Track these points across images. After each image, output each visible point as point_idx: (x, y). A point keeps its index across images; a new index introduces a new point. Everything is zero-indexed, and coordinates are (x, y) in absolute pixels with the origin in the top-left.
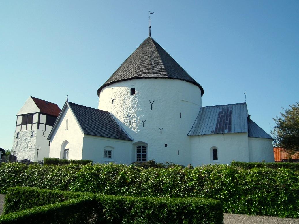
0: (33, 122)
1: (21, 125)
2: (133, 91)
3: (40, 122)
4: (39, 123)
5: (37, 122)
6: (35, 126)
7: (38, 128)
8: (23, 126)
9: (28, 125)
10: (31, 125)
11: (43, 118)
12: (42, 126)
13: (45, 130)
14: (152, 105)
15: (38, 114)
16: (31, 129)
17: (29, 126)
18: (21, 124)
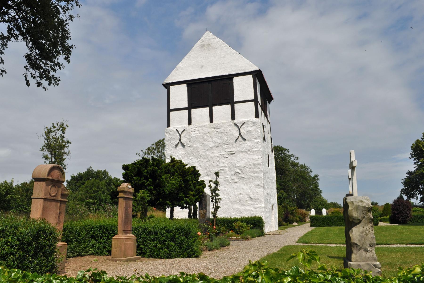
0: (236, 99)
3: (253, 103)
5: (253, 97)
7: (257, 116)
8: (193, 111)
9: (215, 108)
10: (228, 107)
15: (250, 77)
16: (233, 118)
18: (186, 106)
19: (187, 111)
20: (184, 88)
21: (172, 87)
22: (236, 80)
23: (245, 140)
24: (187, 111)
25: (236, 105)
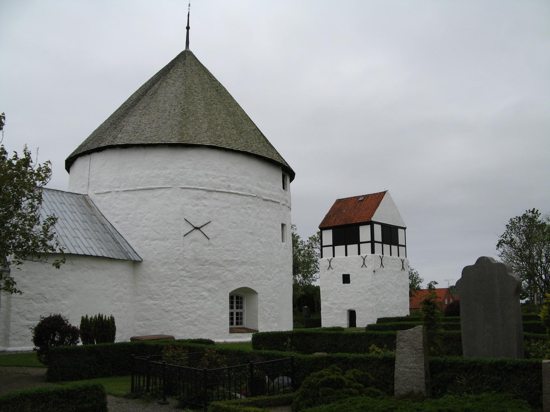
0: (361, 240)
1: (333, 246)
4: (373, 242)
5: (370, 240)
6: (366, 248)
7: (373, 252)
9: (348, 246)
10: (357, 245)
13: (383, 254)
16: (359, 254)
17: (353, 248)
18: (332, 244)
19: (332, 247)
24: (332, 247)
25: (361, 245)
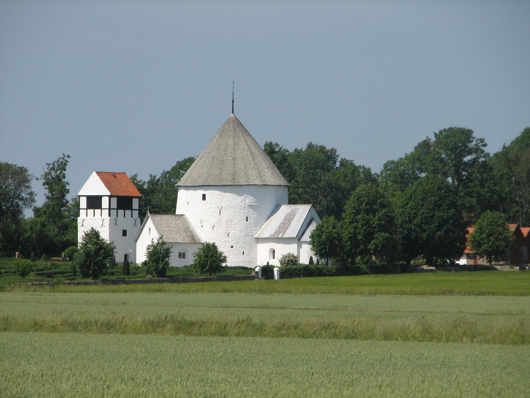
1: (87, 209)
2: (204, 197)
4: (110, 209)
5: (108, 207)
6: (106, 212)
7: (109, 215)
8: (88, 210)
10: (100, 210)
11: (114, 201)
12: (114, 212)
13: (117, 216)
14: (220, 211)
17: (98, 211)
18: (86, 208)
20: (85, 198)
21: (81, 197)
22: (103, 198)
23: (104, 226)
